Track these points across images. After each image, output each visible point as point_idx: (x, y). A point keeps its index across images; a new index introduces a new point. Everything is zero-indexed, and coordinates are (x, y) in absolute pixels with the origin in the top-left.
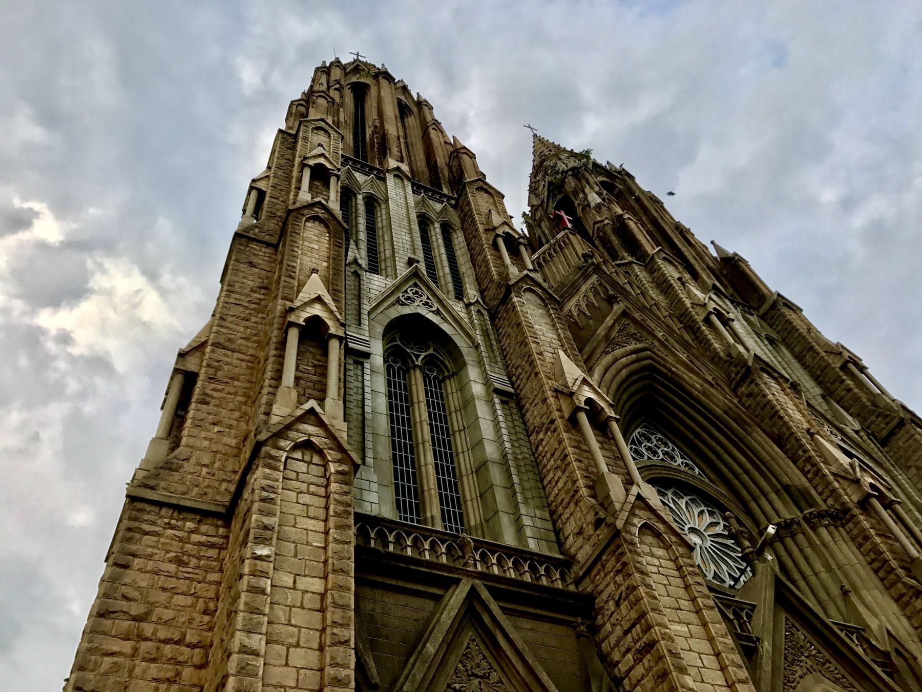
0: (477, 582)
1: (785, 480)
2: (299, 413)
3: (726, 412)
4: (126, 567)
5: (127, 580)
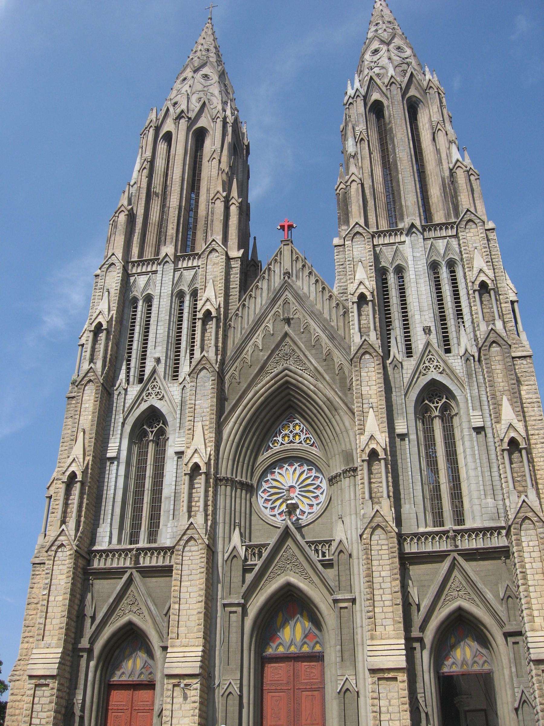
0: (134, 571)
1: (343, 446)
2: (59, 532)
4: (32, 588)
5: (33, 592)
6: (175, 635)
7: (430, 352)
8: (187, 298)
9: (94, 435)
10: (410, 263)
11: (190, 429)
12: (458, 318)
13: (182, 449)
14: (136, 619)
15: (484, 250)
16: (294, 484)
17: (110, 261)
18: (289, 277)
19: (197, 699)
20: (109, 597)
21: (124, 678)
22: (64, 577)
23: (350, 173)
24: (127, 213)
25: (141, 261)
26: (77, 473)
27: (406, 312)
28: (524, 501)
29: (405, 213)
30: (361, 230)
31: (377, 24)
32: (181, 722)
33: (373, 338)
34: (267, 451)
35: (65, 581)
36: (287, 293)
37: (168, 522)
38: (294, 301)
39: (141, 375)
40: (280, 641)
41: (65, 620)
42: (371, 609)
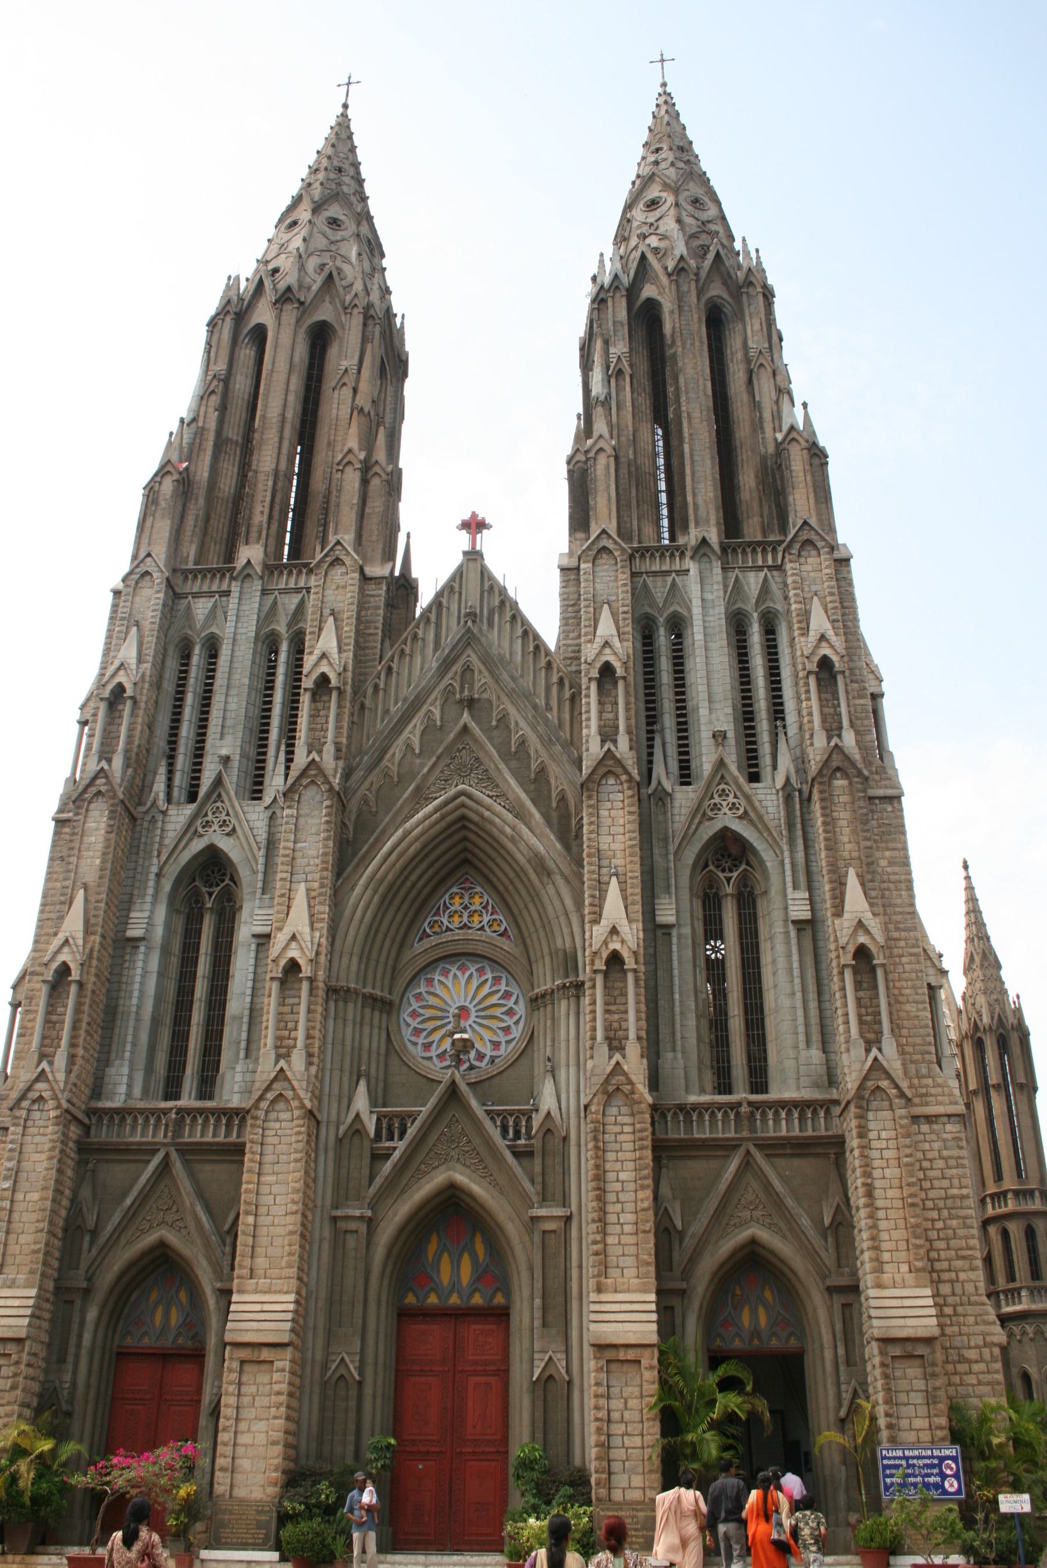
1: (559, 943)
2: (35, 1075)
3: (529, 861)
6: (246, 1272)
7: (723, 777)
8: (284, 647)
9: (104, 896)
10: (696, 611)
11: (282, 896)
12: (776, 719)
13: (266, 930)
14: (172, 1238)
15: (828, 599)
16: (467, 1004)
17: (143, 568)
18: (474, 622)
19: (284, 1387)
20: (125, 1195)
21: (146, 1341)
22: (44, 1156)
23: (596, 435)
24: (176, 477)
25: (200, 571)
26: (72, 965)
27: (684, 701)
28: (876, 1059)
29: (691, 518)
30: (610, 545)
31: (657, 150)
32: (253, 1429)
33: (623, 745)
34: (421, 939)
35: (45, 1164)
36: (469, 651)
37: (237, 1060)
38: (482, 667)
39: (192, 786)
40: (433, 1285)
41: (43, 1237)
42: (598, 1237)
